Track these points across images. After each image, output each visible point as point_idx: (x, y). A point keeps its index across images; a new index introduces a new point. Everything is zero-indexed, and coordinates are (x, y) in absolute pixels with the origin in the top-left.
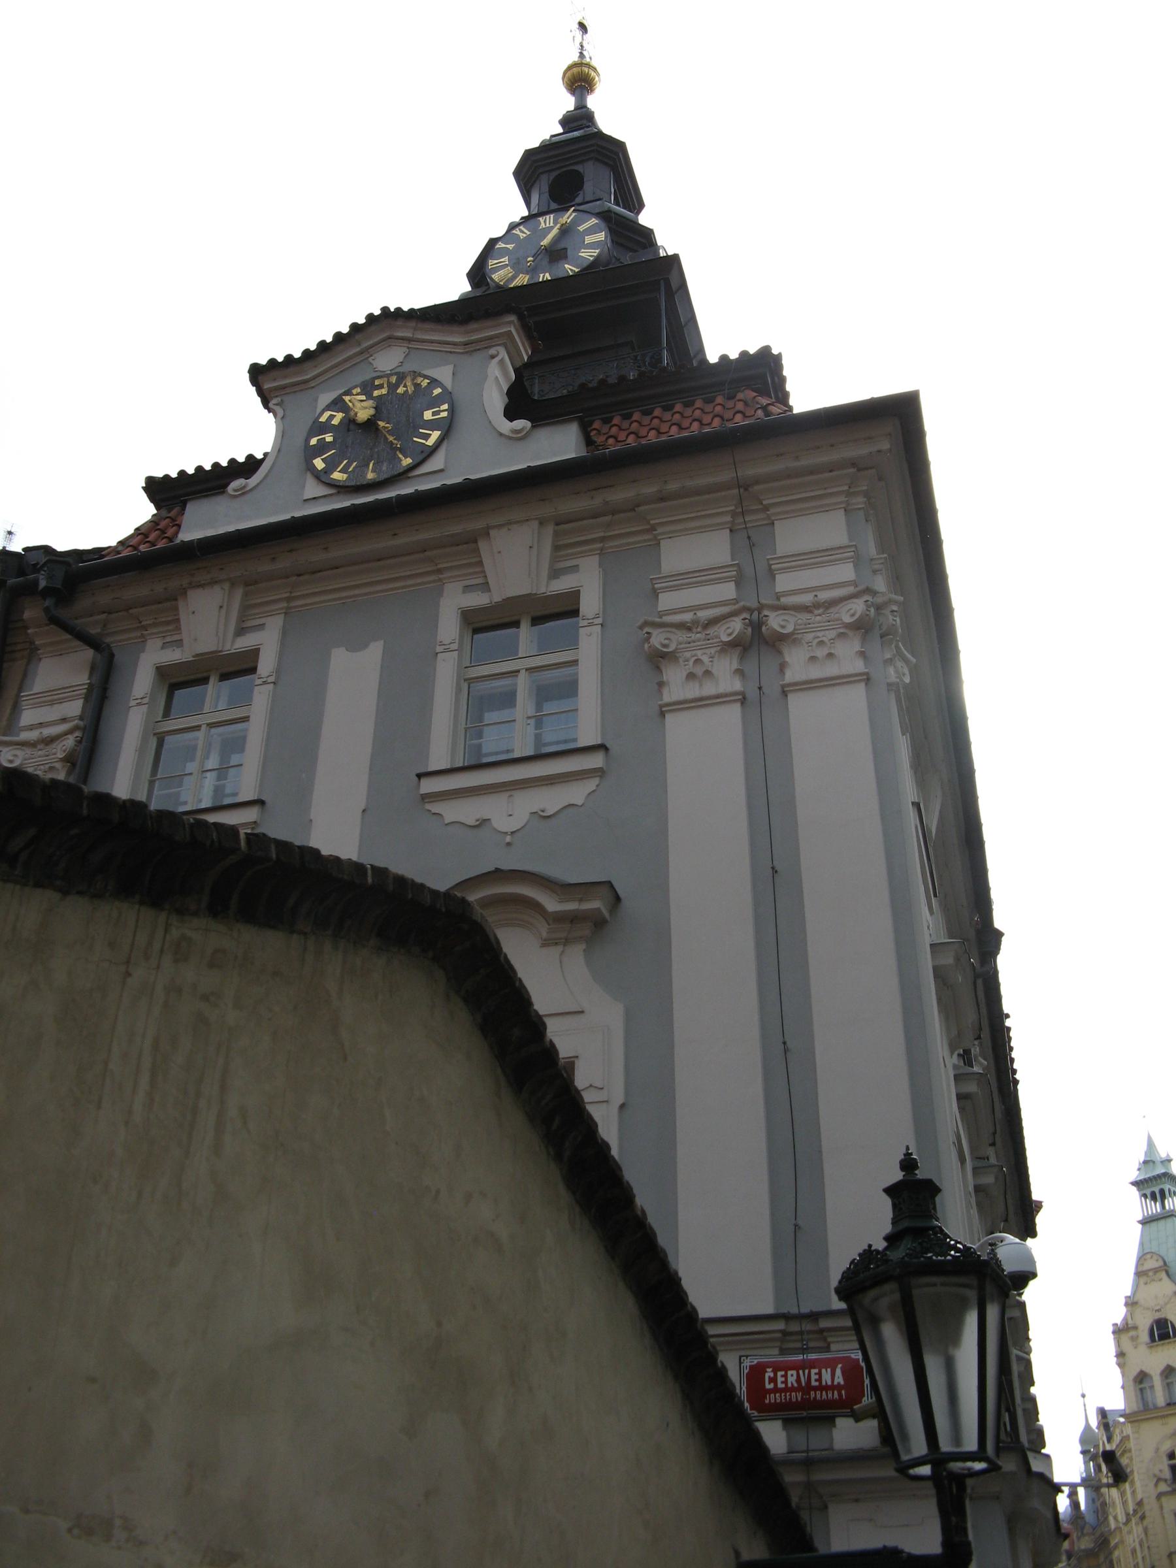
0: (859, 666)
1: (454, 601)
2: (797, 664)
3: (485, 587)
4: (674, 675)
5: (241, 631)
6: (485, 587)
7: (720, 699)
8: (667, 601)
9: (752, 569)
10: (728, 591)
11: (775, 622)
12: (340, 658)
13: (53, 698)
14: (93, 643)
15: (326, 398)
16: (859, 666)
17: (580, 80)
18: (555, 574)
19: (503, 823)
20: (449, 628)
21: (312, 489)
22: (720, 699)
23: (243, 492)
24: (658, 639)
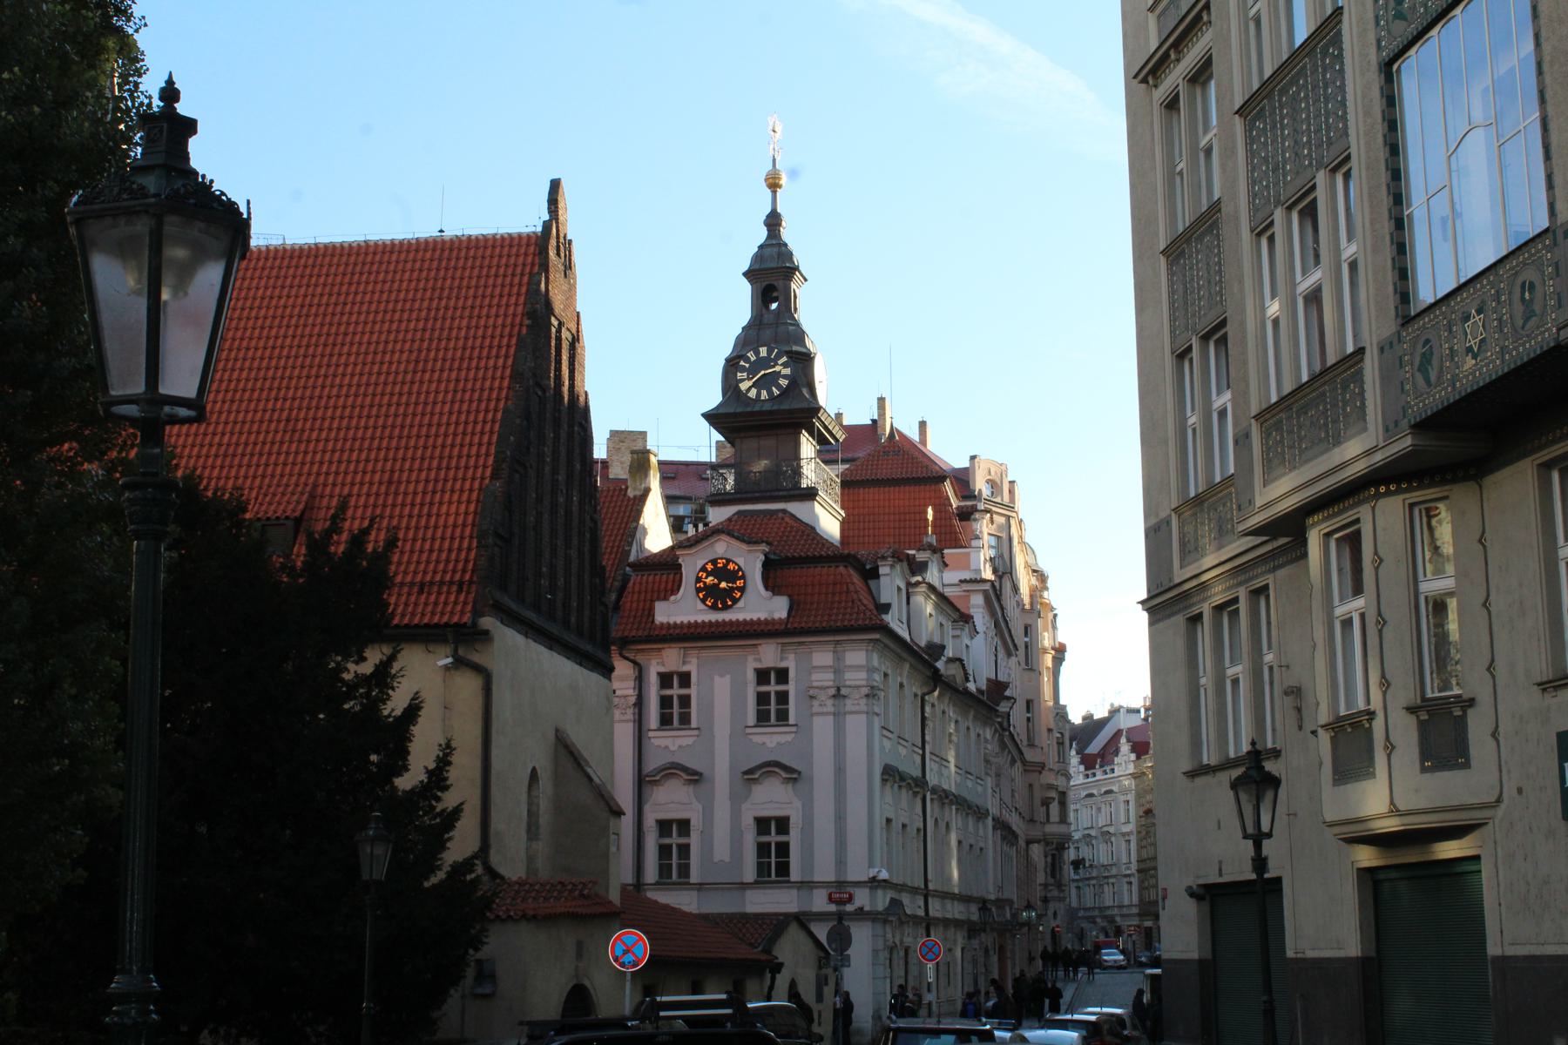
0: (864, 708)
1: (751, 665)
2: (849, 705)
3: (759, 660)
4: (816, 703)
5: (684, 663)
6: (759, 660)
7: (827, 714)
8: (814, 677)
9: (838, 670)
10: (831, 676)
11: (843, 691)
12: (717, 678)
13: (622, 679)
14: (635, 663)
15: (700, 564)
16: (864, 708)
17: (773, 185)
18: (782, 659)
19: (770, 745)
20: (751, 676)
21: (701, 606)
22: (827, 714)
23: (675, 602)
24: (811, 692)
